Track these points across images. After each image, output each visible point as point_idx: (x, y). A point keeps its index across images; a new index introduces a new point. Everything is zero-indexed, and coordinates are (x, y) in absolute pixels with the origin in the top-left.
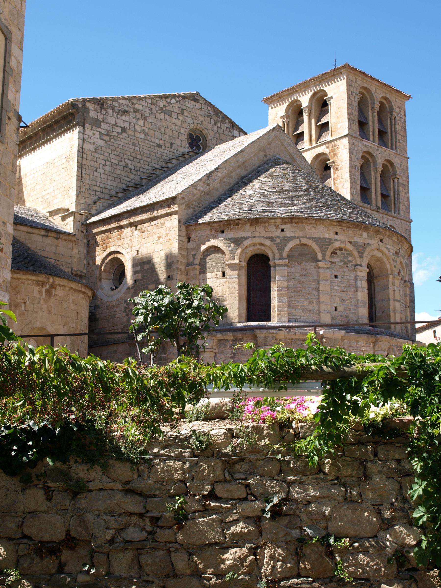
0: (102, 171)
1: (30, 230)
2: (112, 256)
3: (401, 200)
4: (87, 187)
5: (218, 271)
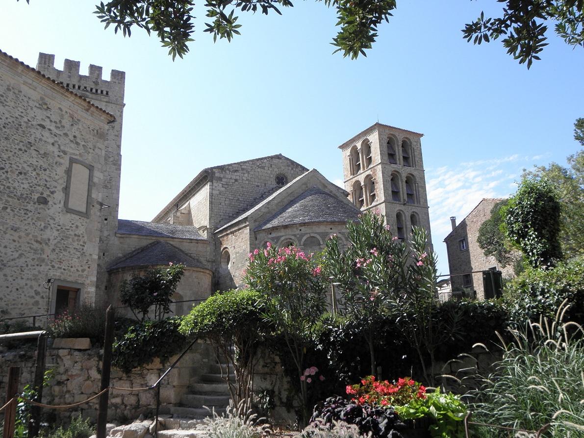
0: (224, 204)
1: (182, 240)
4: (215, 213)
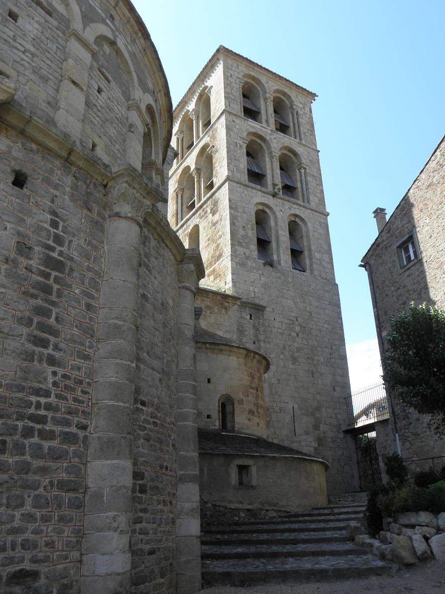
3: (310, 191)
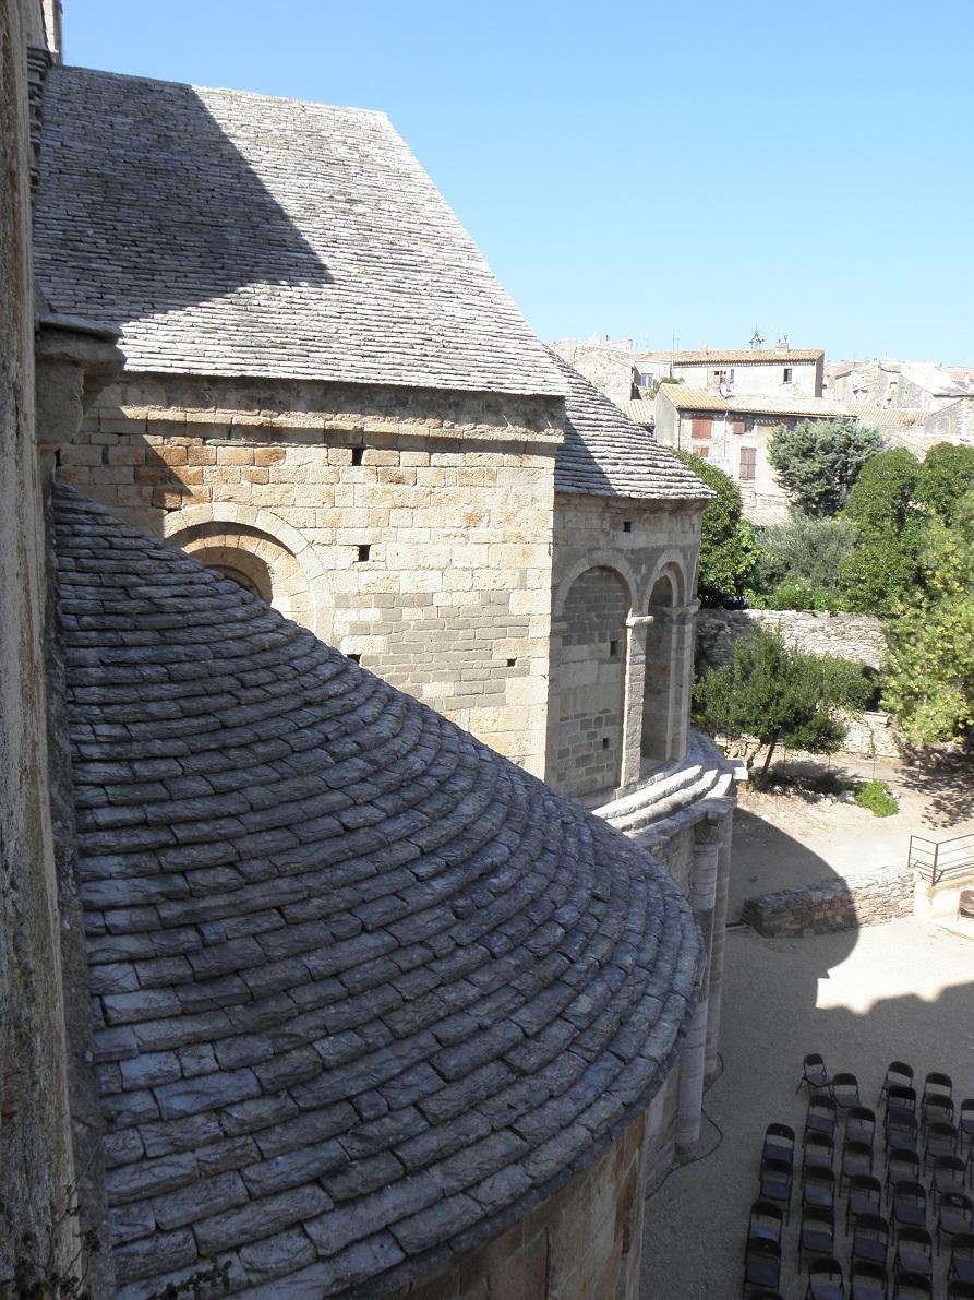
2: (214, 542)
5: (602, 639)
